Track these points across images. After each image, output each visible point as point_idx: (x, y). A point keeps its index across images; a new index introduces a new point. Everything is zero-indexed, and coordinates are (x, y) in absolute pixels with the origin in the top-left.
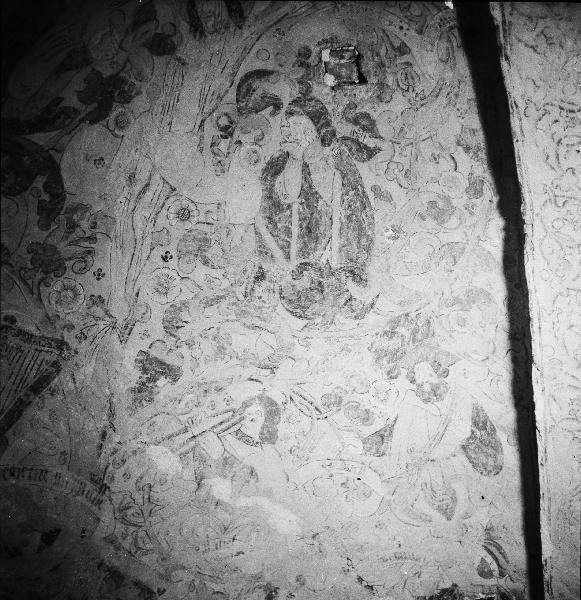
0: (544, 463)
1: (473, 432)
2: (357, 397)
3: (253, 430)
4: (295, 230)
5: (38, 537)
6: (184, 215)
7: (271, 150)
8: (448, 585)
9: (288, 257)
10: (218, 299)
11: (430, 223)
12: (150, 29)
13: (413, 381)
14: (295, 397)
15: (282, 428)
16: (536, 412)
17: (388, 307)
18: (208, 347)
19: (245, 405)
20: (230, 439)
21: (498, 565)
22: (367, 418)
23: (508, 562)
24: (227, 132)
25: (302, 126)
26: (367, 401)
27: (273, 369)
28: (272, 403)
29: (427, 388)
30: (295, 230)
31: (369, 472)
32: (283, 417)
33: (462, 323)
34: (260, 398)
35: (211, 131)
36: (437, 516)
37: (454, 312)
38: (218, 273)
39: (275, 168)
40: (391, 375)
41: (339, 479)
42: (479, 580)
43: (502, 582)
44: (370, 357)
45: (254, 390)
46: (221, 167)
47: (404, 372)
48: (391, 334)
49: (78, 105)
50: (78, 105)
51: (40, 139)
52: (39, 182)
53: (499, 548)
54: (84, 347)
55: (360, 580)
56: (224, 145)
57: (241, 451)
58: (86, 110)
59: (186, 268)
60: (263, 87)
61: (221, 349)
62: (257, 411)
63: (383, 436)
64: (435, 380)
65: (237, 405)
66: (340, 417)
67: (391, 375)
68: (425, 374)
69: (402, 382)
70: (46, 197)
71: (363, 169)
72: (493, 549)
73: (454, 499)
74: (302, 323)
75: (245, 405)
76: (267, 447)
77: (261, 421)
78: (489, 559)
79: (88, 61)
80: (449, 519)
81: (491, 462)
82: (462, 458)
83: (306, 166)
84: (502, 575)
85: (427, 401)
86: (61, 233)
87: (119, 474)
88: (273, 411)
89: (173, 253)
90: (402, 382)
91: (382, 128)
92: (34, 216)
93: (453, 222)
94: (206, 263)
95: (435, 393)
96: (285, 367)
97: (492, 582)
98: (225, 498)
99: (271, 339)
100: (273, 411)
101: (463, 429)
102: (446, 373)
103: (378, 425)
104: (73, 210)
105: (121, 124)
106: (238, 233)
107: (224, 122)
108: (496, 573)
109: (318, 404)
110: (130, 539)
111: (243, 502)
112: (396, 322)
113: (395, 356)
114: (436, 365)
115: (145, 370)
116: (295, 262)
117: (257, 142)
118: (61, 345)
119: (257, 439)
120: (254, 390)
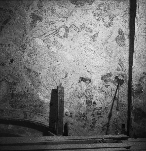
0: (135, 43)
1: (118, 35)
2: (89, 26)
3: (62, 34)
5: (9, 61)
8: (109, 72)
13: (104, 22)
14: (73, 26)
15: (69, 34)
16: (135, 30)
19: (60, 28)
20: (56, 37)
21: (122, 68)
22: (91, 31)
23: (124, 67)
26: (92, 27)
27: (67, 18)
28: (67, 27)
29: (107, 24)
31: (91, 45)
32: (70, 31)
33: (118, 6)
34: (64, 26)
40: (98, 20)
41: (84, 47)
42: (117, 71)
43: (122, 72)
44: (93, 15)
45: (62, 24)
47: (102, 19)
48: (99, 9)
53: (122, 64)
54: (17, 12)
55: (88, 71)
57: (59, 40)
62: (63, 29)
63: (95, 36)
64: (109, 22)
65: (57, 28)
67: (98, 20)
68: (107, 20)
69: (101, 22)
72: (121, 64)
73: (112, 52)
74: (75, 5)
75: (60, 28)
76: (66, 39)
77: (64, 32)
78: (120, 67)
80: (110, 57)
81: (122, 43)
82: (115, 42)
84: (122, 70)
85: (107, 27)
87: (28, 45)
88: (67, 30)
90: (101, 22)
95: (110, 25)
97: (120, 72)
98: (55, 52)
99: (66, 10)
100: (67, 30)
101: (116, 34)
102: (113, 20)
103: (94, 33)
108: (121, 70)
109: (79, 27)
110: (32, 61)
111: (59, 53)
112: (100, 6)
113: (99, 15)
114: (110, 17)
115: (33, 18)
118: (11, 11)
119: (63, 37)
120: (62, 24)
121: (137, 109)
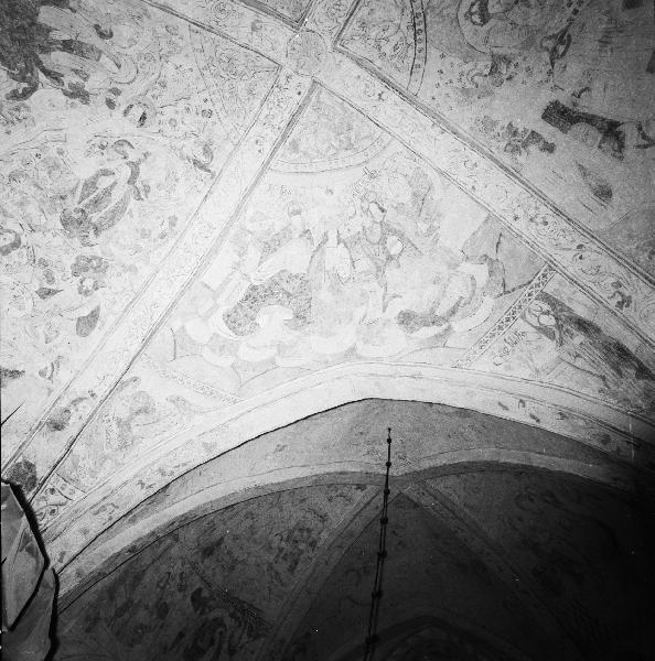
4: (92, 197)
6: (61, 152)
7: (108, 166)
9: (79, 203)
10: (39, 188)
11: (139, 235)
12: (112, 97)
15: (14, 253)
17: (97, 251)
18: (18, 198)
19: (9, 231)
22: (51, 280)
24: (102, 147)
25: (127, 172)
26: (57, 276)
28: (20, 242)
30: (92, 197)
31: (30, 301)
35: (97, 141)
36: (43, 339)
37: (120, 269)
38: (50, 181)
39: (105, 173)
41: (15, 292)
45: (18, 229)
46: (88, 153)
49: (66, 85)
50: (66, 85)
51: (42, 76)
52: (25, 85)
56: (97, 149)
58: (66, 87)
59: (41, 166)
60: (126, 148)
61: (22, 204)
63: (50, 293)
66: (40, 272)
67: (75, 274)
68: (88, 283)
69: (77, 280)
70: (20, 91)
71: (133, 201)
75: (9, 231)
77: (8, 242)
78: (50, 368)
79: (85, 79)
82: (75, 322)
83: (115, 183)
86: (10, 106)
88: (16, 244)
89: (42, 158)
90: (77, 280)
91: (150, 195)
92: (9, 90)
93: (146, 240)
94: (50, 173)
95: (86, 293)
96: (38, 235)
99: (43, 220)
100: (16, 244)
101: (86, 312)
103: (53, 287)
104: (27, 108)
105: (72, 105)
106: (71, 177)
107: (105, 144)
112: (95, 258)
116: (80, 206)
117: (108, 160)
121: (27, 463)
